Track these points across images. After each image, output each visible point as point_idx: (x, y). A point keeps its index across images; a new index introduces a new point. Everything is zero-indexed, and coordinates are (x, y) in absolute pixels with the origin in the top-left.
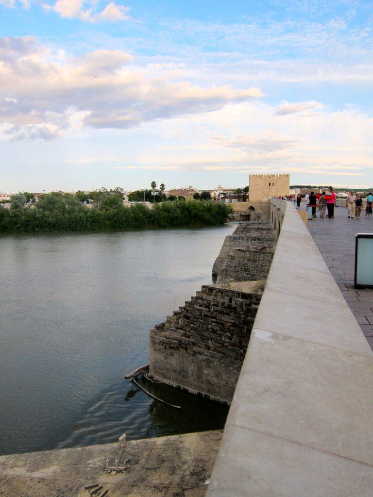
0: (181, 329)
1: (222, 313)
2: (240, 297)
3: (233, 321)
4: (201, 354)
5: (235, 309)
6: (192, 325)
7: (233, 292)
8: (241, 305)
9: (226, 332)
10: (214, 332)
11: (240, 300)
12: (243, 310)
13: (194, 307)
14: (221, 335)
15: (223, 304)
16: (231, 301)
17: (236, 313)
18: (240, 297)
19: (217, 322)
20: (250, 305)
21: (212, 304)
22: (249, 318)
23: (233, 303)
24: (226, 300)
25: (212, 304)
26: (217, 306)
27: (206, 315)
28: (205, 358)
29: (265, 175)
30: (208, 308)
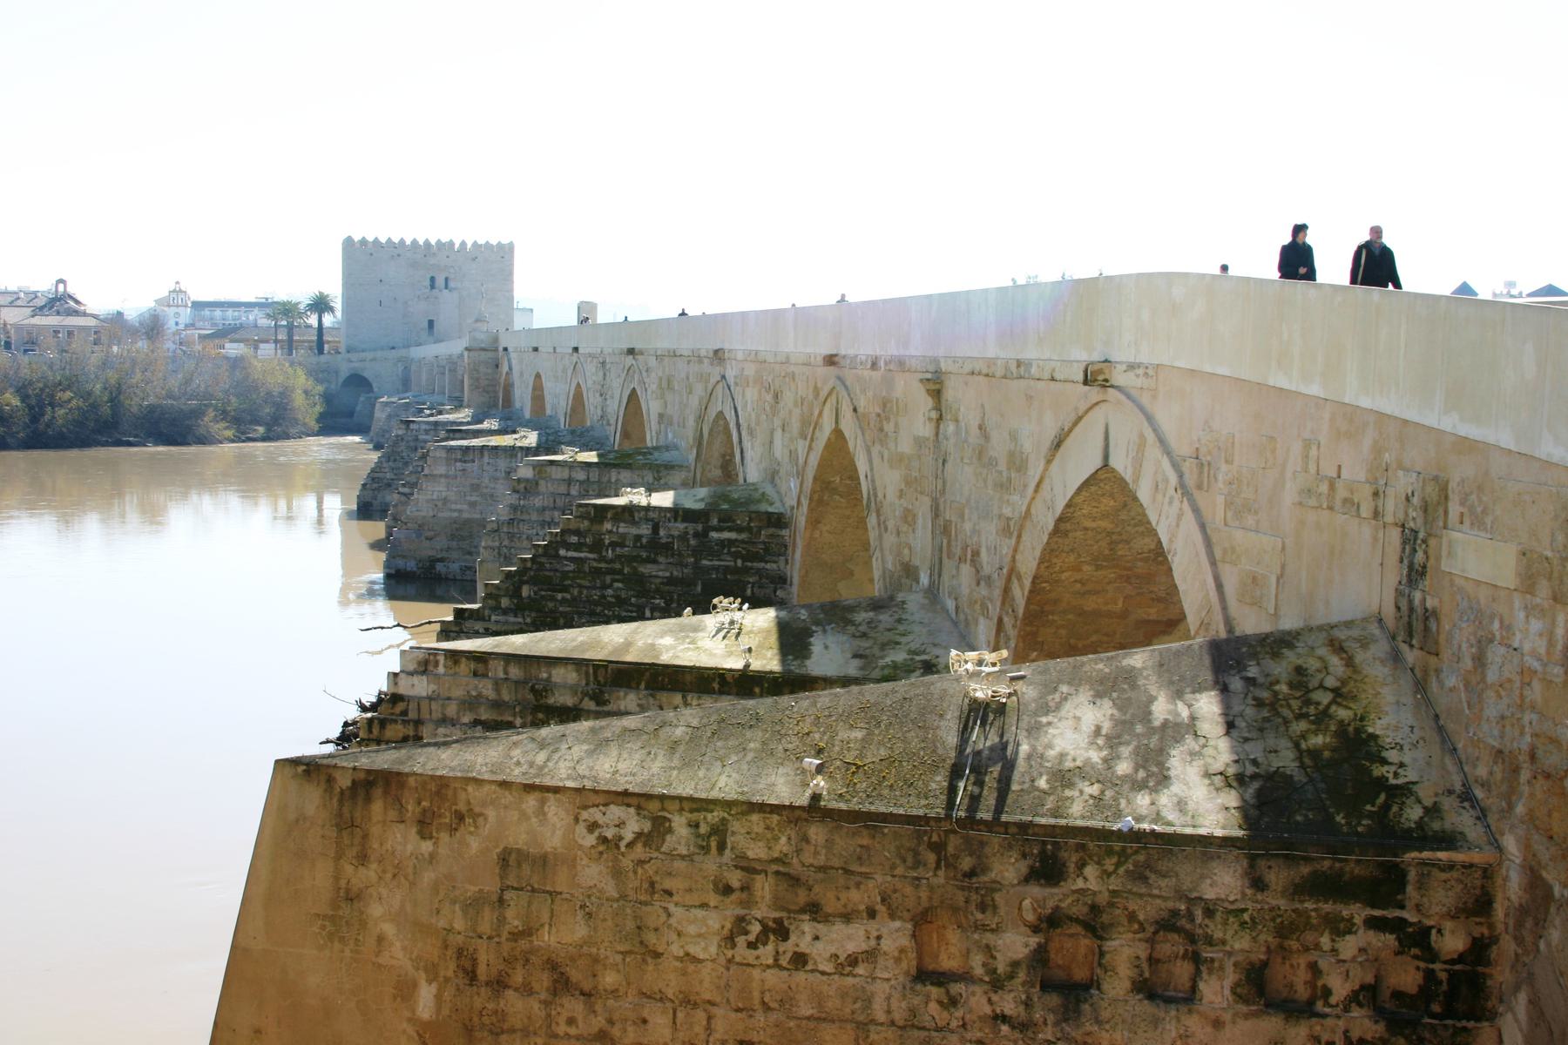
2: (679, 519)
3: (668, 574)
5: (667, 547)
6: (559, 596)
8: (683, 537)
9: (655, 598)
11: (681, 526)
12: (688, 546)
13: (557, 556)
15: (638, 538)
16: (656, 529)
17: (673, 555)
18: (679, 519)
20: (705, 533)
21: (607, 542)
22: (705, 562)
23: (662, 533)
25: (607, 542)
26: (622, 545)
27: (596, 568)
29: (415, 242)
30: (600, 553)
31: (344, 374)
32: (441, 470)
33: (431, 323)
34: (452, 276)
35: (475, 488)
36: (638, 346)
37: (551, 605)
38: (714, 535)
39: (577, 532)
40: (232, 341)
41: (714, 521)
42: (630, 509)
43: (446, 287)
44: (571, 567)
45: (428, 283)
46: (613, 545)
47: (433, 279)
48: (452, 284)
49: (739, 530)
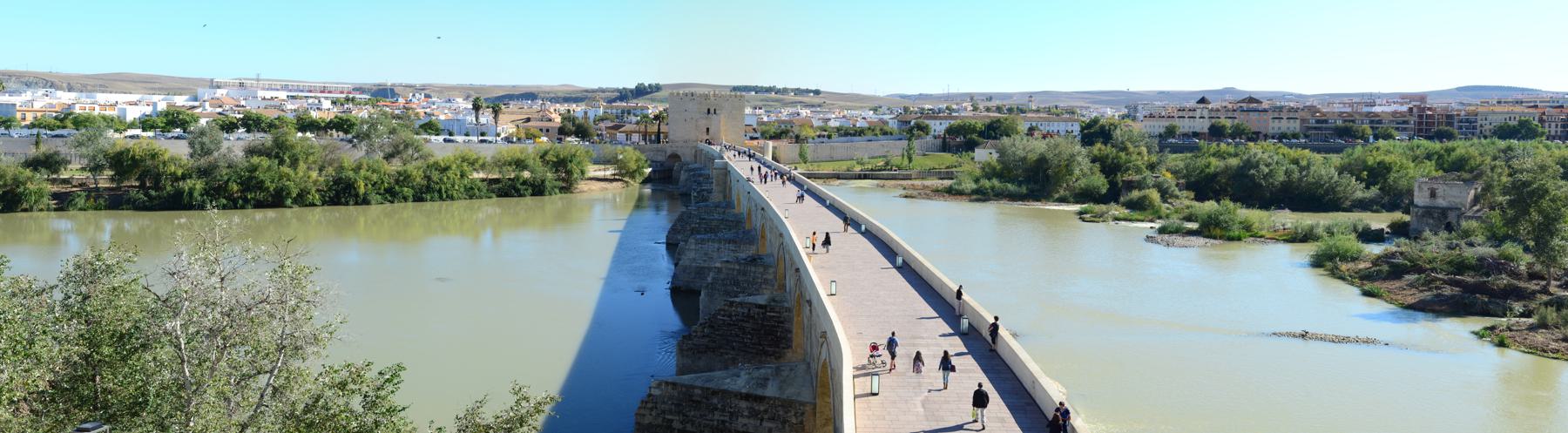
0: (707, 336)
1: (743, 321)
4: (727, 354)
7: (750, 303)
8: (758, 314)
10: (737, 336)
11: (757, 310)
14: (743, 339)
15: (743, 313)
16: (749, 310)
19: (739, 329)
23: (751, 311)
24: (746, 311)
28: (731, 356)
31: (669, 153)
32: (693, 247)
33: (708, 129)
34: (717, 108)
35: (706, 254)
36: (766, 209)
37: (714, 336)
38: (768, 314)
39: (724, 310)
40: (620, 132)
41: (768, 309)
42: (741, 304)
43: (715, 113)
44: (721, 322)
45: (706, 111)
46: (735, 315)
47: (709, 110)
48: (717, 112)
49: (777, 312)
